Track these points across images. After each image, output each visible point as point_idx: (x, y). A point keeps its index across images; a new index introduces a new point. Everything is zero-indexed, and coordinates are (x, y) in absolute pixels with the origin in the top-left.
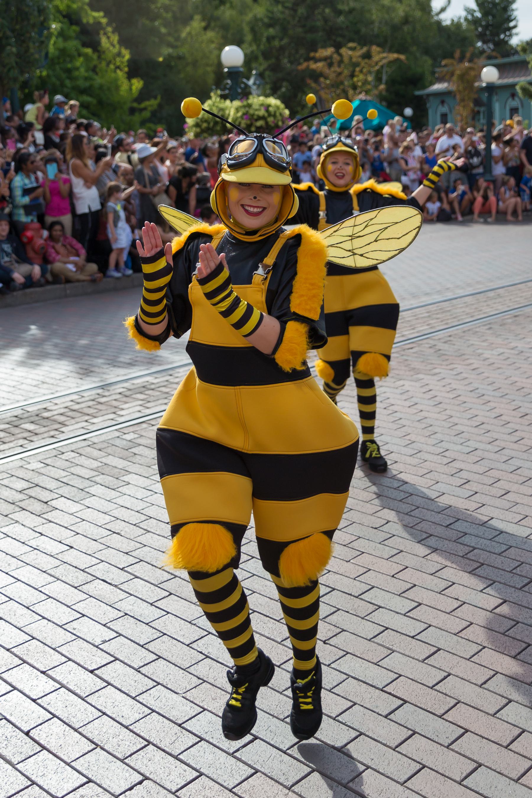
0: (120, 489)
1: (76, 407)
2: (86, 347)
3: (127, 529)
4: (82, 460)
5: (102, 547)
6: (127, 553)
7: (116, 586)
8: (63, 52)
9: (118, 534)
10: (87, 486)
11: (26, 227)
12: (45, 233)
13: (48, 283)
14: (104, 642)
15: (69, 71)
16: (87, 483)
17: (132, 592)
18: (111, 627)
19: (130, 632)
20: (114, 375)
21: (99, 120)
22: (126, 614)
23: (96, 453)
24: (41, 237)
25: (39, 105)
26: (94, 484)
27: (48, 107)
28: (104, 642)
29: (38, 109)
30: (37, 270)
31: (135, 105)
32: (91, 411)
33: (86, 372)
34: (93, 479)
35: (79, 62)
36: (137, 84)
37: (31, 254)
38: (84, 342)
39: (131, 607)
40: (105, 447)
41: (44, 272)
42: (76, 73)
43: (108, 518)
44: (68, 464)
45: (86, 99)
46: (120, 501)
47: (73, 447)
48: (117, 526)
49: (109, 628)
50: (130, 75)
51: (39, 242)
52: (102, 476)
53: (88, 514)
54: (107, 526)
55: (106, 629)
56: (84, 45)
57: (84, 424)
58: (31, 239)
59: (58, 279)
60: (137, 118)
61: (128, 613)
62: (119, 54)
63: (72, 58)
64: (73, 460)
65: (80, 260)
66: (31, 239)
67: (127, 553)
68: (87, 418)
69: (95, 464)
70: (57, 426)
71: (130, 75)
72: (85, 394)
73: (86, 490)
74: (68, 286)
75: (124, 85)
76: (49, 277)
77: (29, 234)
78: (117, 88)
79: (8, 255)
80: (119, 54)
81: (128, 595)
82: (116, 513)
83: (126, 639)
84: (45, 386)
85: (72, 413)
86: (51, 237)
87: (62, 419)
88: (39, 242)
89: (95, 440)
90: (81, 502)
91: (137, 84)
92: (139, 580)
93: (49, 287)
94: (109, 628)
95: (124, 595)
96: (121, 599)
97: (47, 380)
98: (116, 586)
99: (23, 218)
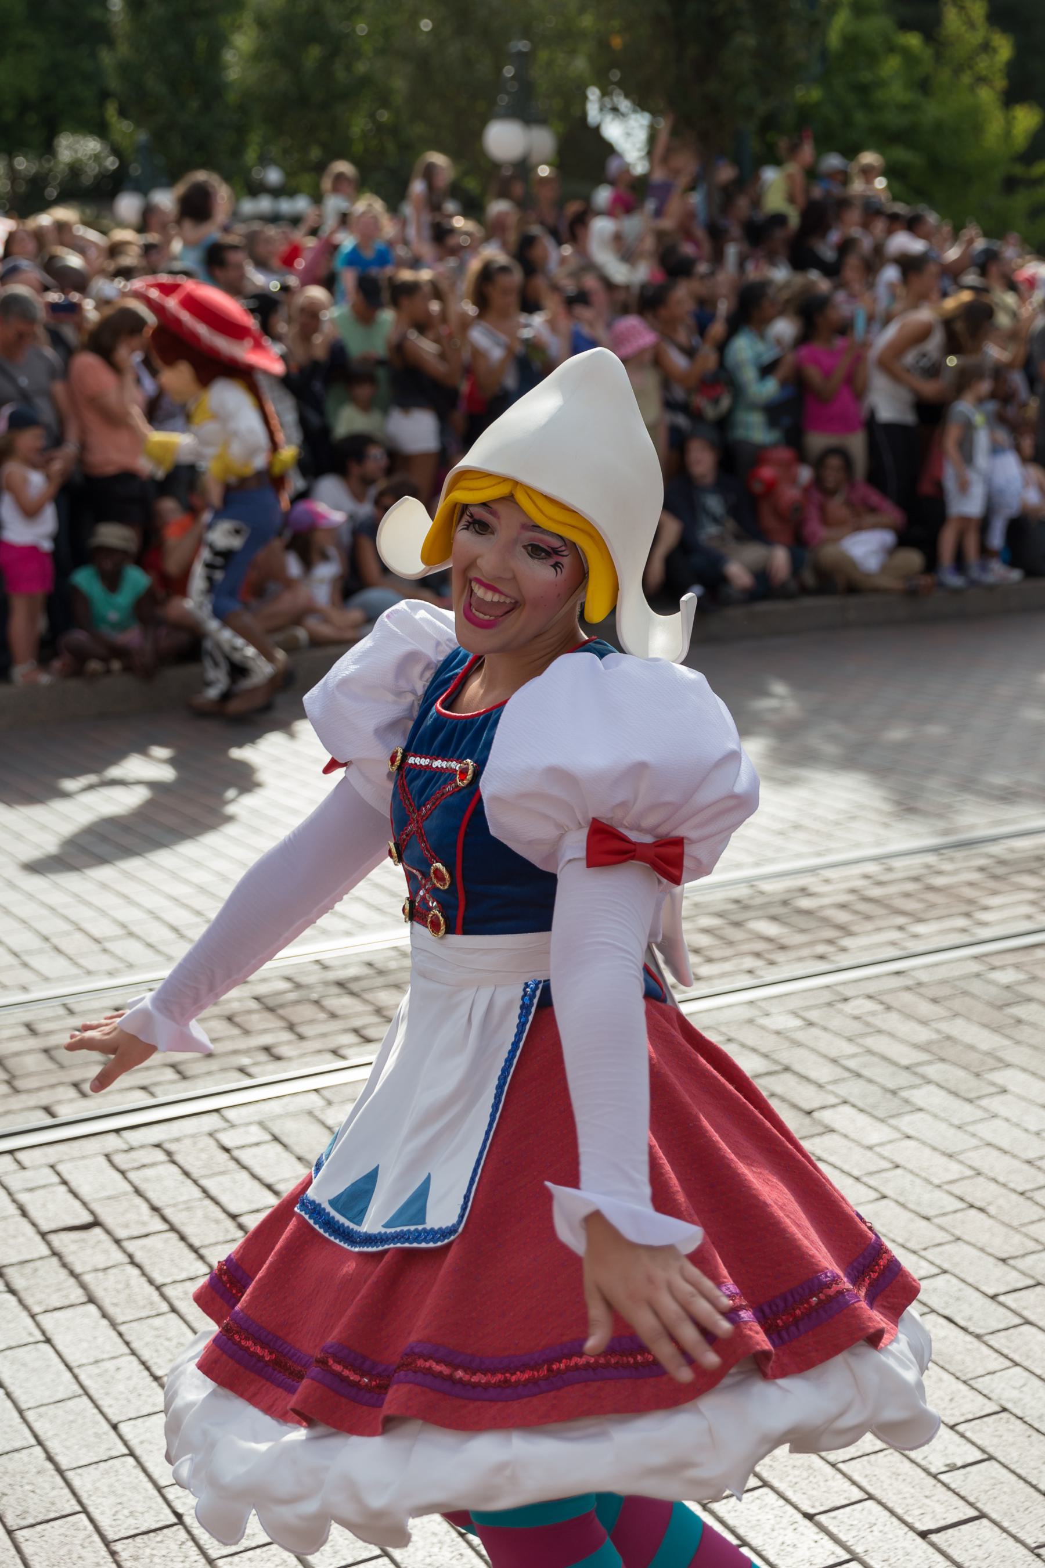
0: (984, 1102)
1: (876, 892)
2: (904, 747)
3: (1001, 1201)
4: (892, 1021)
5: (941, 1236)
6: (1004, 1260)
7: (978, 1337)
8: (851, 41)
9: (981, 1210)
10: (904, 1083)
11: (759, 455)
12: (805, 474)
13: (804, 591)
14: (952, 1468)
15: (863, 90)
16: (904, 1079)
17: (1017, 1358)
18: (968, 1434)
19: (1015, 1455)
20: (977, 818)
21: (934, 206)
22: (1004, 1410)
23: (925, 1008)
24: (793, 480)
25: (793, 168)
26: (918, 1081)
27: (812, 174)
28: (952, 1468)
29: (790, 178)
30: (780, 558)
31: (1018, 170)
32: (910, 905)
33: (908, 806)
34: (921, 1070)
35: (892, 64)
36: (1026, 120)
37: (769, 521)
38: (897, 734)
39: (1015, 1394)
40: (947, 995)
41: (796, 564)
42: (880, 95)
43: (955, 1170)
44: (857, 1027)
45: (902, 154)
46: (985, 1130)
47: (872, 988)
48: (980, 1191)
49: (962, 1436)
50: (1011, 98)
51: (790, 494)
52: (940, 1066)
53: (906, 1152)
54: (957, 1189)
55: (956, 1438)
56: (905, 26)
57: (895, 935)
58: (771, 486)
59: (838, 583)
60: (1021, 201)
61: (1008, 1406)
62: (986, 47)
63: (873, 58)
64: (870, 1019)
65: (883, 538)
66: (771, 486)
67: (1004, 1260)
68: (901, 920)
69: (923, 1035)
70: (830, 933)
71: (1011, 98)
72: (897, 863)
73: (904, 1094)
74: (853, 601)
75: (995, 125)
76: (809, 578)
77: (767, 472)
78: (978, 129)
79: (716, 520)
80: (986, 47)
81: (1008, 1363)
82: (975, 1158)
83: (1004, 1471)
84: (801, 835)
85: (868, 905)
86: (818, 482)
87: (842, 917)
88: (790, 494)
89: (924, 976)
90: (893, 1122)
91: (1026, 120)
92: (1034, 1330)
93: (808, 602)
94: (962, 1436)
95: (996, 1362)
96: (991, 1368)
97: (806, 822)
98: (978, 1337)
99: (755, 429)
